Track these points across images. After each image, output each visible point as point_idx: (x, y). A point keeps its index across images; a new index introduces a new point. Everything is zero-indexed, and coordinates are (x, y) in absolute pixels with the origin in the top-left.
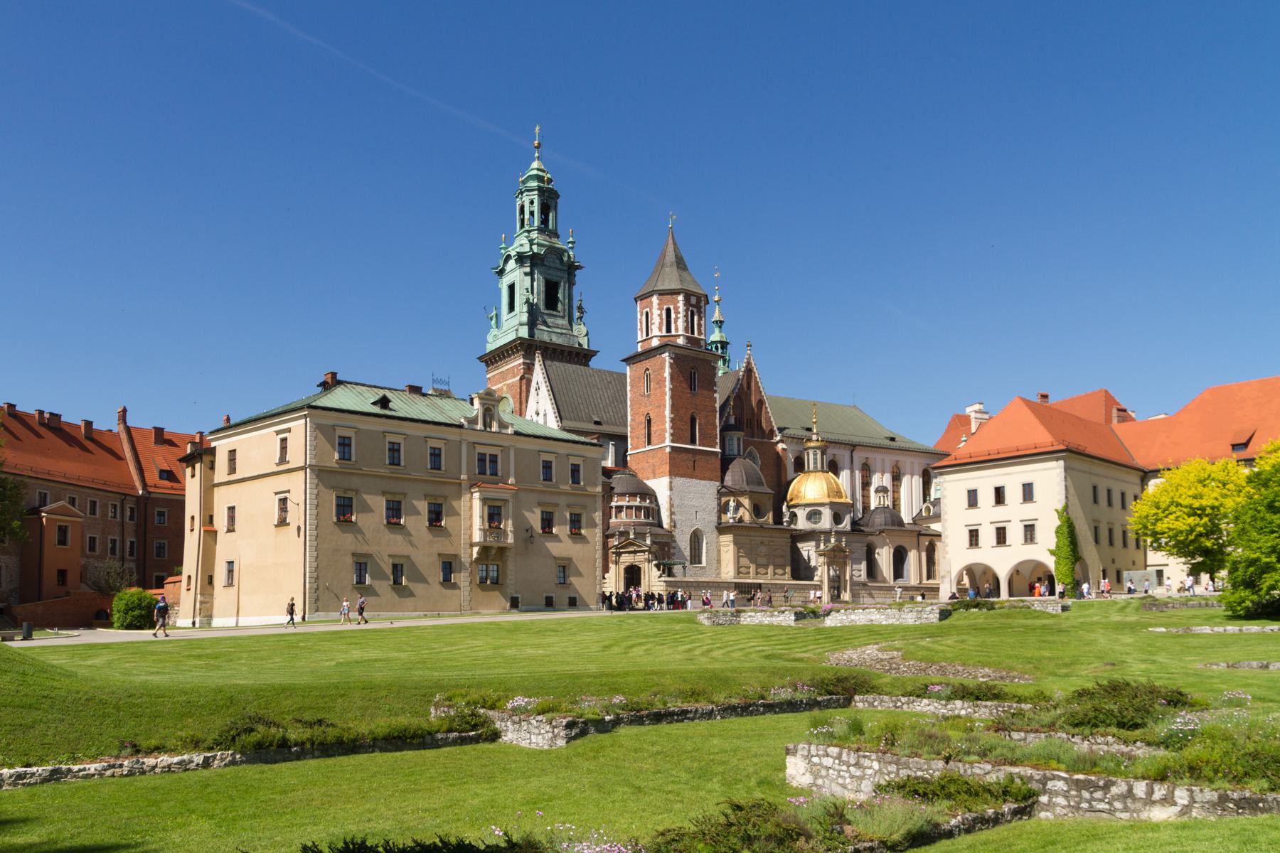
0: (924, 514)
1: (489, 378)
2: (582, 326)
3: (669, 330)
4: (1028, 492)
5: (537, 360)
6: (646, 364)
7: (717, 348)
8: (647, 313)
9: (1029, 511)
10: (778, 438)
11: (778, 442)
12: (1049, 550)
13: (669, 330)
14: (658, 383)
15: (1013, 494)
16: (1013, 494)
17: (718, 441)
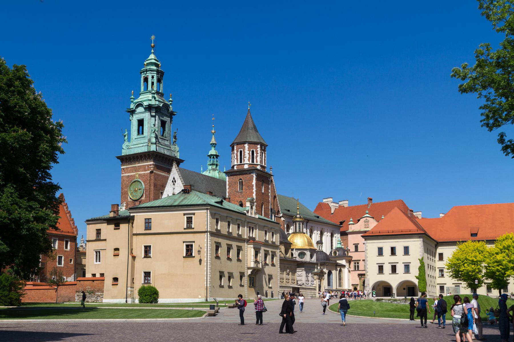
0: (333, 255)
1: (123, 169)
2: (176, 146)
3: (253, 161)
4: (406, 250)
5: (174, 166)
6: (241, 177)
7: (213, 158)
8: (241, 152)
9: (407, 259)
10: (281, 215)
11: (281, 217)
12: (416, 276)
13: (253, 161)
14: (248, 187)
15: (400, 251)
16: (400, 251)
17: (270, 217)
